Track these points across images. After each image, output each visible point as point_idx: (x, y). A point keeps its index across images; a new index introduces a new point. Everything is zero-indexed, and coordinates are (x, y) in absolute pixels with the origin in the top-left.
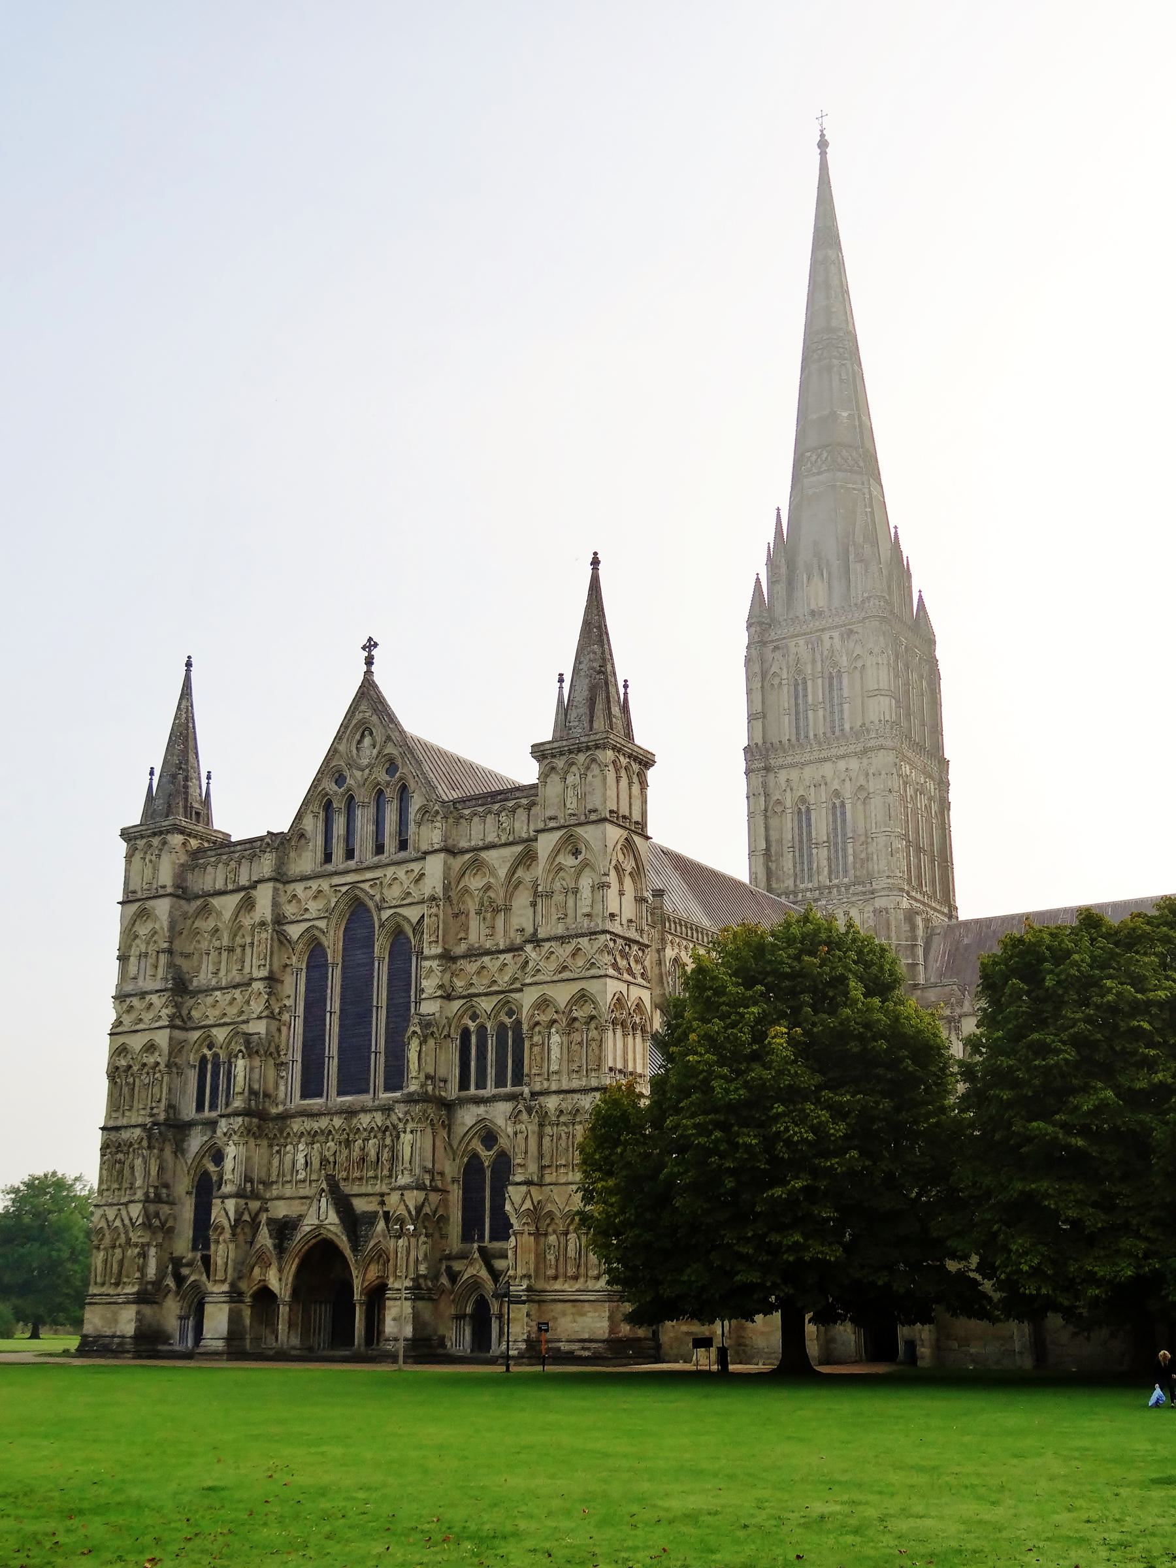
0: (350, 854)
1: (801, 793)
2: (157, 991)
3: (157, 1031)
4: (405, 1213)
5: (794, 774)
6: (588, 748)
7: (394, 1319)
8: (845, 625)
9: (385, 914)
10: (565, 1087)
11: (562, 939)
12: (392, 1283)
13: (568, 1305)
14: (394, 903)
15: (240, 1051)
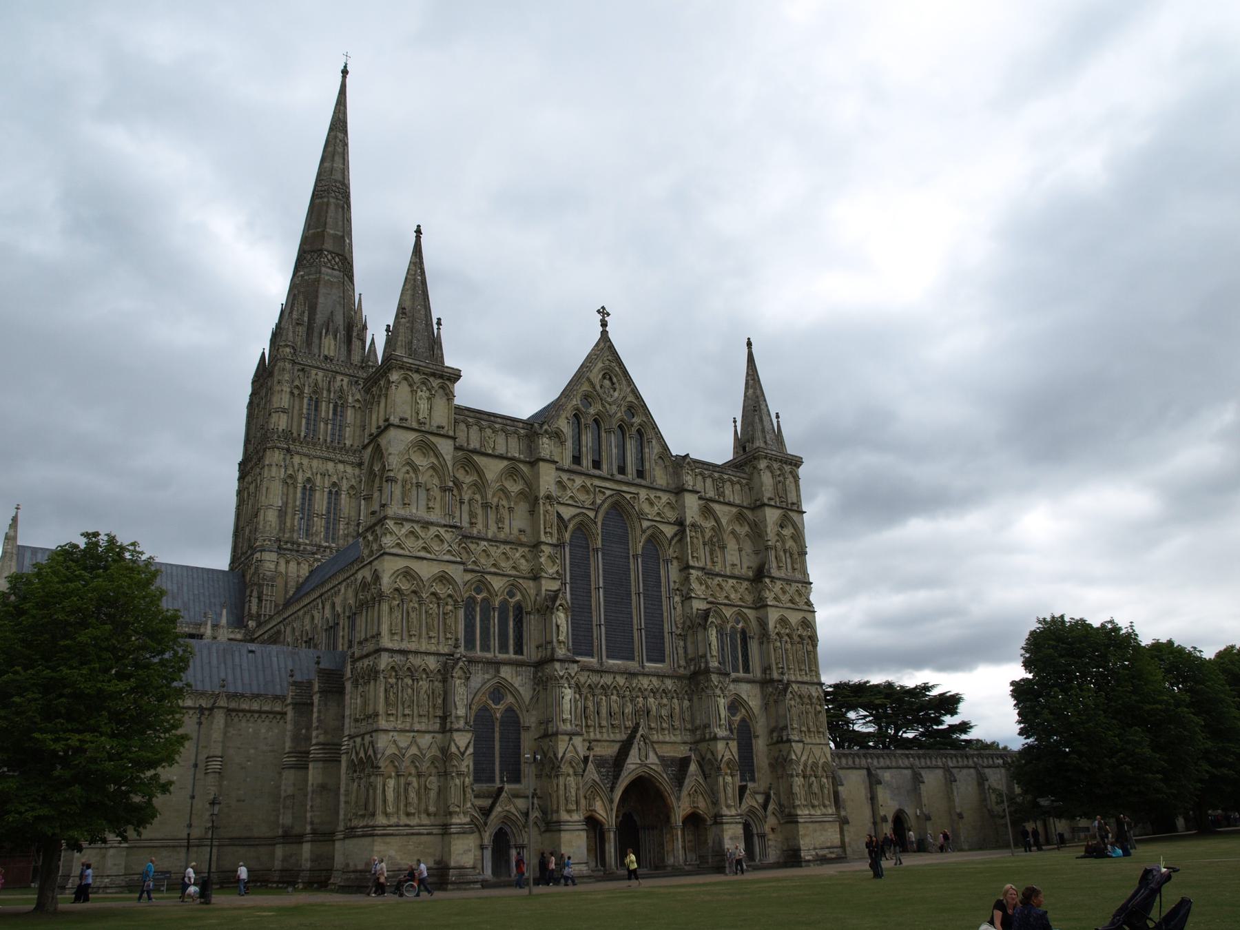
0: (597, 464)
1: (309, 475)
2: (445, 526)
3: (447, 563)
4: (731, 757)
5: (305, 461)
6: (791, 464)
7: (731, 838)
8: (356, 377)
9: (645, 524)
10: (800, 679)
11: (789, 581)
12: (725, 811)
13: (817, 824)
14: (650, 517)
15: (560, 605)
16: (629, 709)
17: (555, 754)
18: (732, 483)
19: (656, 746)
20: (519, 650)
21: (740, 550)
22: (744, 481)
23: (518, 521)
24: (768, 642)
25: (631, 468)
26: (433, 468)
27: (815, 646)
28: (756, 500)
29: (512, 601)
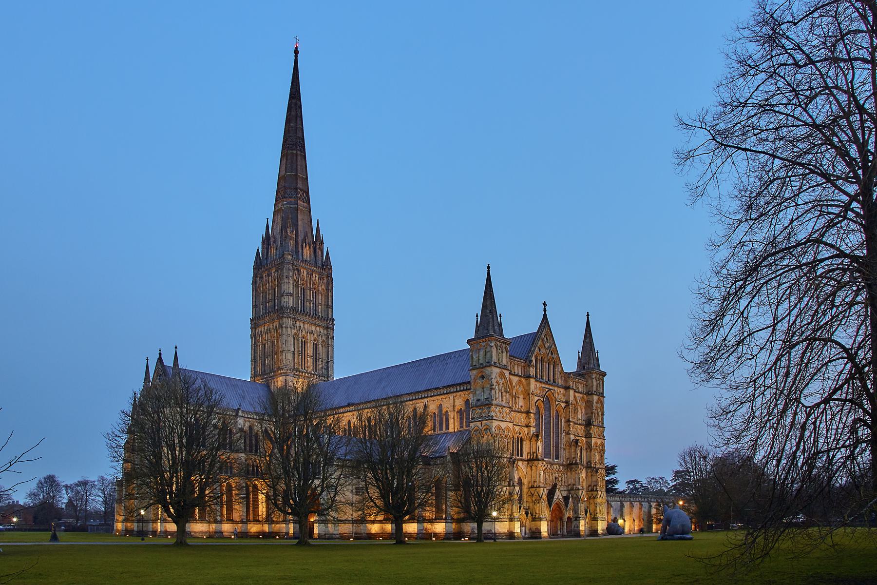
5: (302, 325)
9: (557, 403)
16: (551, 478)
17: (538, 495)
18: (581, 383)
19: (562, 492)
20: (521, 456)
21: (582, 413)
22: (585, 382)
23: (521, 402)
24: (591, 451)
25: (551, 378)
26: (503, 384)
27: (604, 453)
28: (589, 391)
29: (520, 436)
